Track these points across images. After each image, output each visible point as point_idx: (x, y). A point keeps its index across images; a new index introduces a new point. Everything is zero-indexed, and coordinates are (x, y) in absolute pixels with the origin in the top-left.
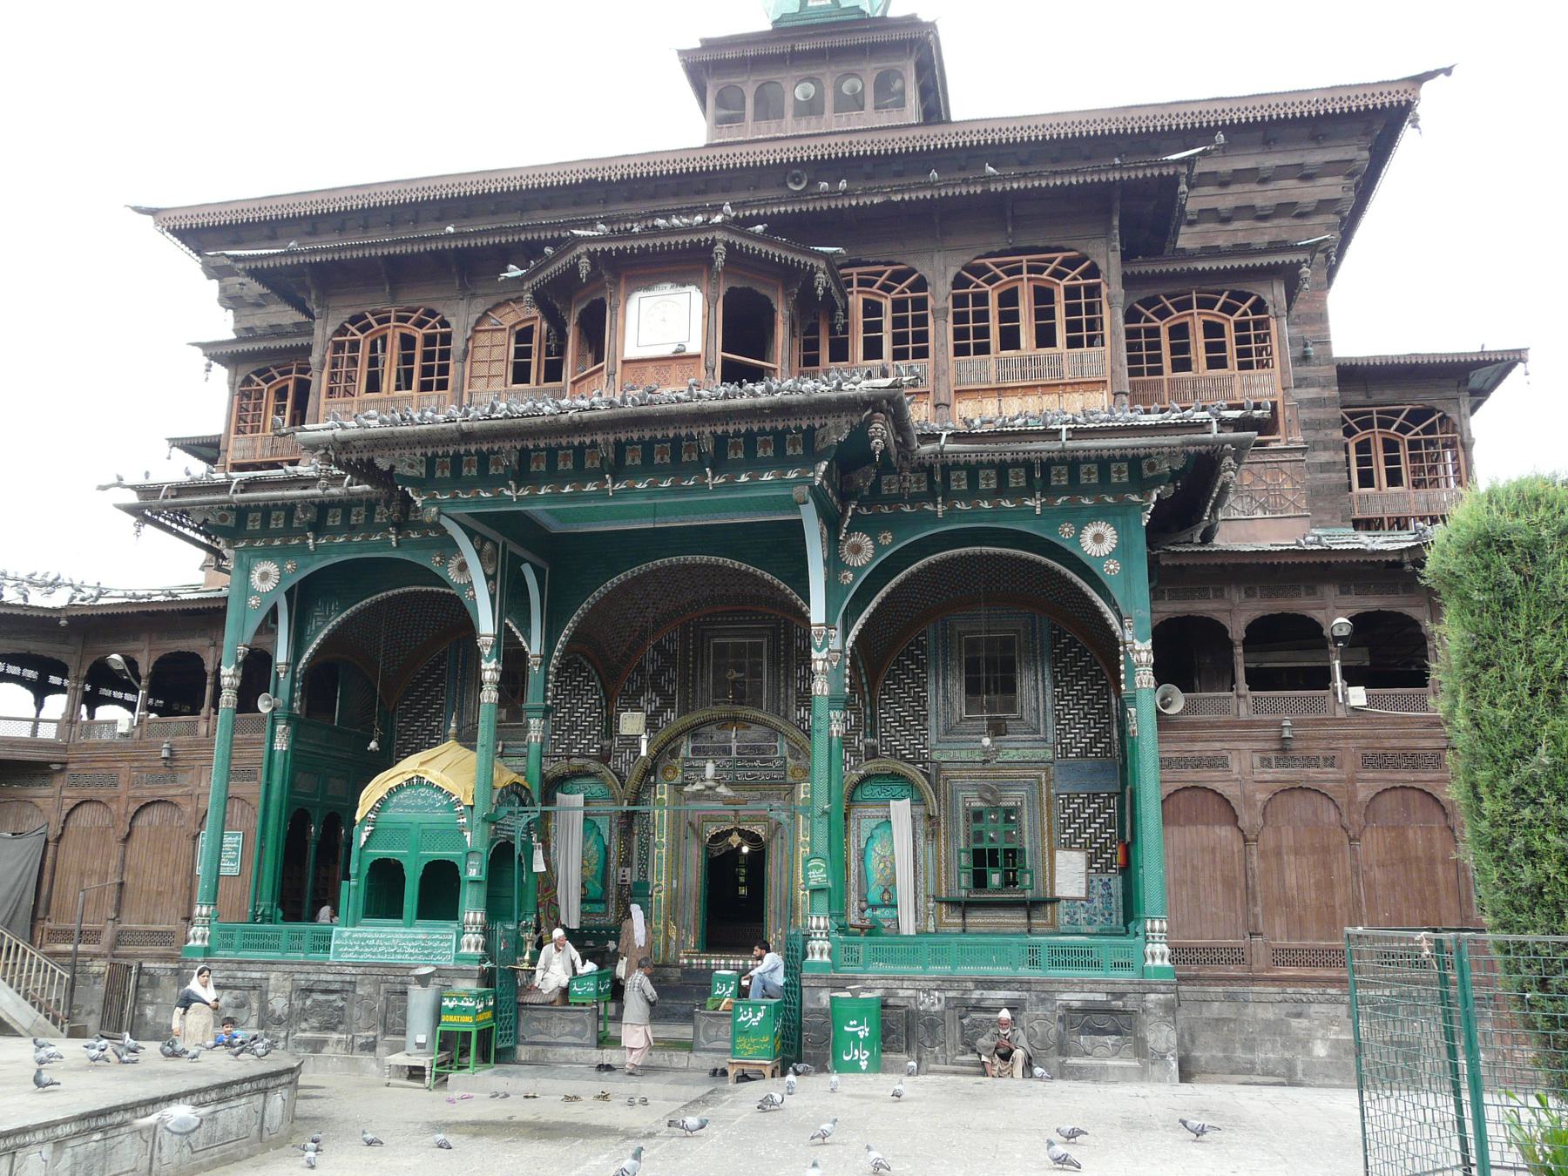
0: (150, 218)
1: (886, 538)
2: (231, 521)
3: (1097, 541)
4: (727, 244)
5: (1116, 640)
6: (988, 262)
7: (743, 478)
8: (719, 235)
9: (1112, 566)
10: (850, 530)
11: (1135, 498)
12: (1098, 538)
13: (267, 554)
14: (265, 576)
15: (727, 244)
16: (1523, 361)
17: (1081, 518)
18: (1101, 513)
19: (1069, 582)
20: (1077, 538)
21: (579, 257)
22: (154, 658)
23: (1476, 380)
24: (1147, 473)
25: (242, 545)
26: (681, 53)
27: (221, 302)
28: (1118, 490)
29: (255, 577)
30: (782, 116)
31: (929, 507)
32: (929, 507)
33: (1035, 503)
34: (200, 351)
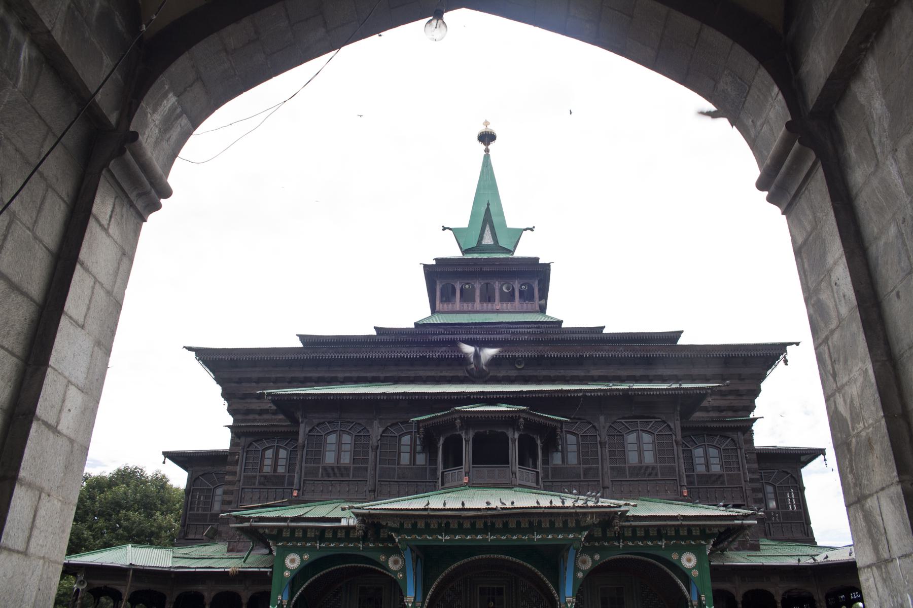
0: (193, 353)
1: (597, 557)
2: (275, 532)
3: (689, 561)
4: (524, 419)
5: (686, 599)
6: (623, 421)
7: (550, 537)
8: (524, 415)
9: (695, 573)
10: (581, 553)
11: (703, 542)
12: (689, 560)
13: (294, 550)
14: (293, 561)
15: (524, 419)
16: (824, 454)
17: (681, 550)
18: (689, 549)
19: (663, 569)
20: (680, 559)
21: (455, 419)
22: (213, 594)
23: (803, 458)
24: (707, 531)
25: (280, 544)
26: (425, 266)
27: (223, 395)
28: (695, 538)
29: (288, 562)
30: (474, 301)
31: (616, 544)
32: (616, 544)
33: (663, 543)
34: (229, 430)
